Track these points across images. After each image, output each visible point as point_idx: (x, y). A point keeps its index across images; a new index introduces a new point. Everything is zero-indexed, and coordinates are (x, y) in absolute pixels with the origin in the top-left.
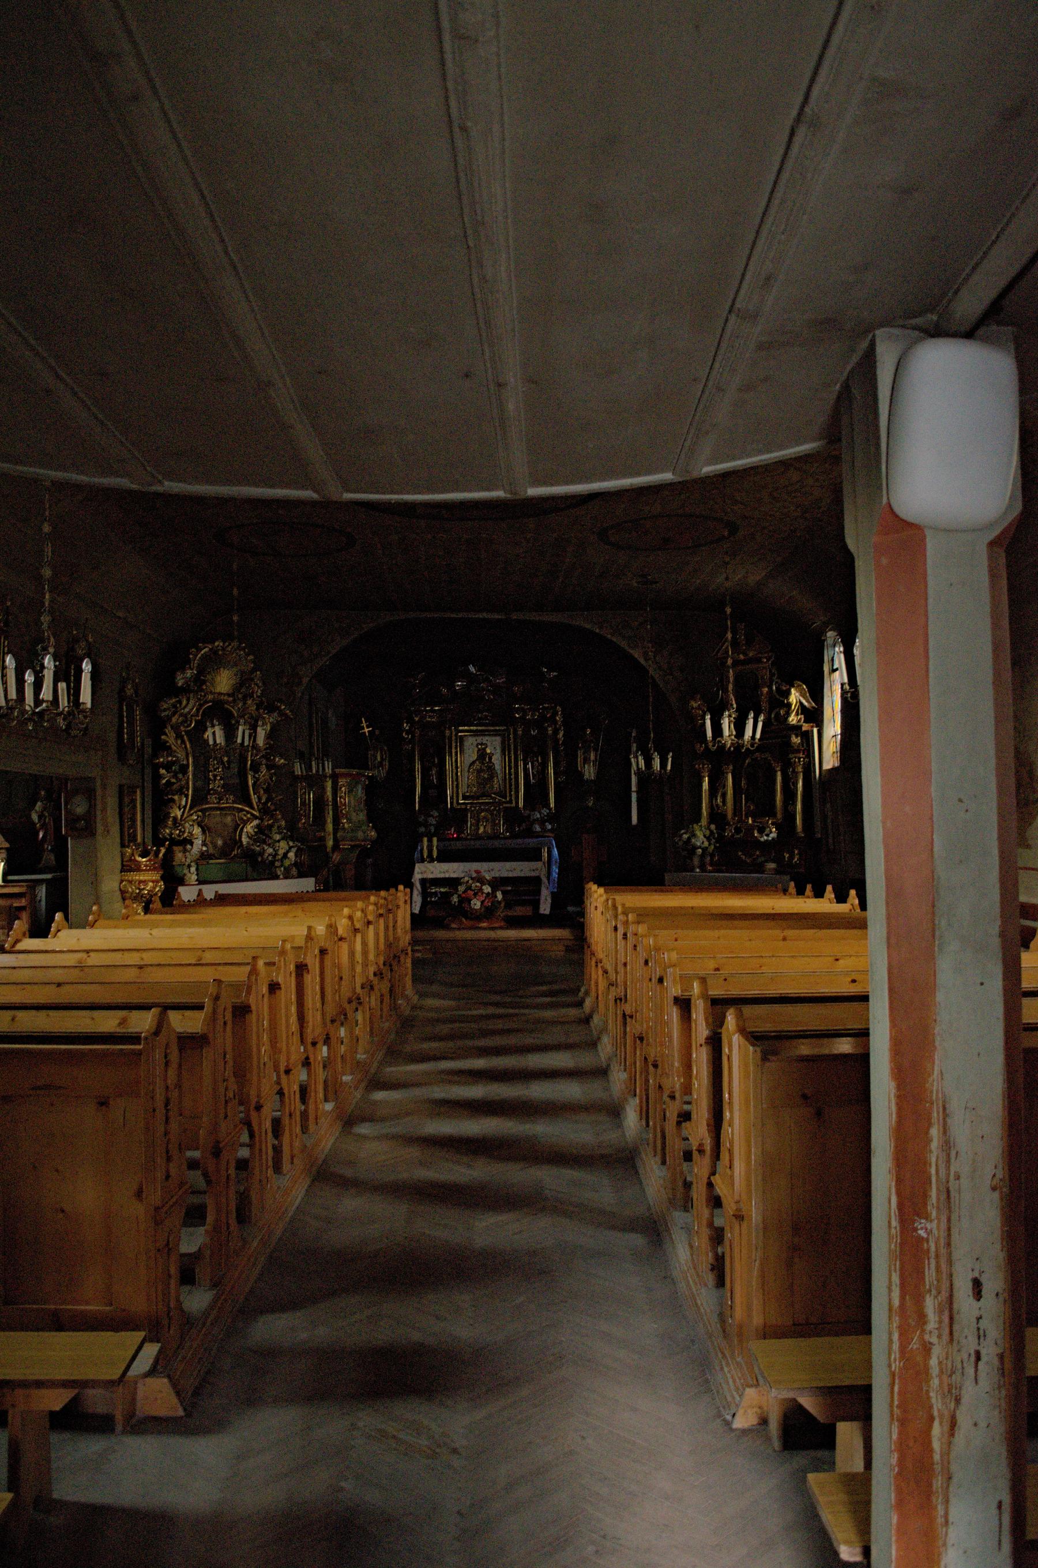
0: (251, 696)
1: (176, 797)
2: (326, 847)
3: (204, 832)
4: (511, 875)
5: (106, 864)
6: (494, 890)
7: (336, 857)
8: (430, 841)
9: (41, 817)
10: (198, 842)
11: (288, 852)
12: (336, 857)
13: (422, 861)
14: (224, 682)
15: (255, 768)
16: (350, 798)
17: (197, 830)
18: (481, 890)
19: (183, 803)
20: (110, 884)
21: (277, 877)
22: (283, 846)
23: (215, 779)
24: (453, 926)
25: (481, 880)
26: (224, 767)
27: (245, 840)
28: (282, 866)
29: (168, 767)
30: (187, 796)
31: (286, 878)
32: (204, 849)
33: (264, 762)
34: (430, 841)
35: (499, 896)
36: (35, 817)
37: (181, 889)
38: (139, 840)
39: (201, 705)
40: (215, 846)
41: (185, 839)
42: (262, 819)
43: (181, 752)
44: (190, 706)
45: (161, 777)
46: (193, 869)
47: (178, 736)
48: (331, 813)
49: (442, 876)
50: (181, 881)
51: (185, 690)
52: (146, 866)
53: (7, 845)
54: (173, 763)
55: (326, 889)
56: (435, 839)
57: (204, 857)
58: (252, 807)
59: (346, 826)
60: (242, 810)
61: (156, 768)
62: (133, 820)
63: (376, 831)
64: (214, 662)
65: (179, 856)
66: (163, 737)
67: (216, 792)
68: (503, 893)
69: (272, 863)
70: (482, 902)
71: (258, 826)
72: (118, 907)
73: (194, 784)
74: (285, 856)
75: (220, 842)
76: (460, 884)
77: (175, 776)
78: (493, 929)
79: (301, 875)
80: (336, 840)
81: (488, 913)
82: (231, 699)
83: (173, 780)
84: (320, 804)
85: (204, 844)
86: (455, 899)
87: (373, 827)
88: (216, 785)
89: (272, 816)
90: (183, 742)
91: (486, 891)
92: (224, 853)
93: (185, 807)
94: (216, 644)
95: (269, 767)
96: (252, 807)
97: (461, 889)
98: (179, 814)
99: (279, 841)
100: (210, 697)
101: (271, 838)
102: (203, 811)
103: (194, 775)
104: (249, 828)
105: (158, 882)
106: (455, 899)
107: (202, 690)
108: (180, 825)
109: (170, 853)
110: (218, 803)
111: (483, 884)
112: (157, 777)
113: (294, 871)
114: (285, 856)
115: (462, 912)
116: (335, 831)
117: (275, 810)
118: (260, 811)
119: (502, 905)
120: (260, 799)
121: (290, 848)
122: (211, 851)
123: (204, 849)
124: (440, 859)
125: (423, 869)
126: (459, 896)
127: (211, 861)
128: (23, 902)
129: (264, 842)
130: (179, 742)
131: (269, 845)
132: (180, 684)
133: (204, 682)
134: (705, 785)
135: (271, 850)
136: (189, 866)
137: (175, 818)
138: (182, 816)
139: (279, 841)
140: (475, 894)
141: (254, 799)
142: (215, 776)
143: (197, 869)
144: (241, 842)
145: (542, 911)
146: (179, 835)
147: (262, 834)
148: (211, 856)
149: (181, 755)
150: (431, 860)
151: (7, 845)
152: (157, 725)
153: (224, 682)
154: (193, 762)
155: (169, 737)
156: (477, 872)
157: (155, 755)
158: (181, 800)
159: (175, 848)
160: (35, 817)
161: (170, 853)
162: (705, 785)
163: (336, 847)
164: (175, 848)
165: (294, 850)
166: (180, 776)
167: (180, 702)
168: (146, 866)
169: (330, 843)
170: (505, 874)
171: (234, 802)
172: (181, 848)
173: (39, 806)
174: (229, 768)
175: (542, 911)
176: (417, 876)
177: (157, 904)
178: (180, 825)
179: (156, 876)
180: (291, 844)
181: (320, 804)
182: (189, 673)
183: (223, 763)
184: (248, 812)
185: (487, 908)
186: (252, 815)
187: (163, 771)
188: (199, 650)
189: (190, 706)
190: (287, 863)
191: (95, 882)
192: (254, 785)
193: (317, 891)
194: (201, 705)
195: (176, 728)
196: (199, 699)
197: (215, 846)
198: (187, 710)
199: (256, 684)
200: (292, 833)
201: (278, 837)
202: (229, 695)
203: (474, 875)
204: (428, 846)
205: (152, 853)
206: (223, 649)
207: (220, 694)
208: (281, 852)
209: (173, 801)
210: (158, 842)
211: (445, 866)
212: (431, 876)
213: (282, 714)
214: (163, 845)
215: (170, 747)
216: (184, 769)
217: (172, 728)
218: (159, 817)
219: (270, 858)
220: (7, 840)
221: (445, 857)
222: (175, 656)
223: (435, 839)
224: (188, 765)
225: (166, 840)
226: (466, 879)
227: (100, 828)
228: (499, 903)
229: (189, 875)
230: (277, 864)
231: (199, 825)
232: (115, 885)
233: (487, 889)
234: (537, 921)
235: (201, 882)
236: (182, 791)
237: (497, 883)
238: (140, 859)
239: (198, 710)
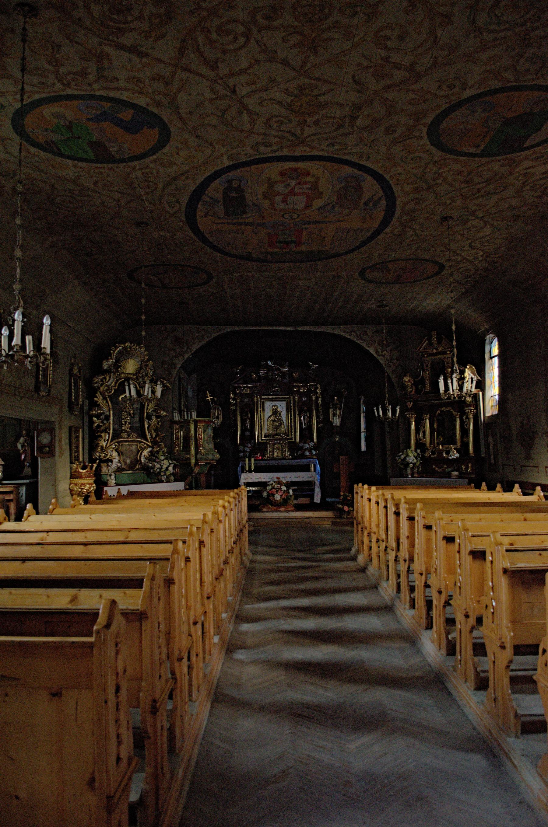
0: (147, 375)
1: (103, 434)
2: (190, 463)
3: (119, 455)
4: (297, 480)
5: (61, 474)
6: (288, 490)
7: (196, 470)
8: (250, 460)
9: (23, 446)
10: (115, 461)
11: (168, 466)
12: (196, 470)
14: (130, 367)
15: (149, 417)
16: (204, 435)
17: (115, 454)
18: (280, 489)
19: (107, 438)
20: (64, 485)
21: (162, 482)
22: (166, 463)
23: (126, 424)
24: (264, 510)
25: (280, 483)
26: (131, 417)
27: (143, 460)
28: (165, 475)
29: (98, 416)
30: (109, 434)
31: (167, 482)
32: (119, 465)
33: (154, 414)
34: (250, 460)
35: (291, 492)
36: (19, 447)
37: (105, 489)
38: (81, 459)
39: (117, 380)
40: (125, 463)
41: (108, 459)
42: (153, 447)
44: (111, 381)
45: (94, 422)
46: (113, 477)
47: (104, 398)
48: (194, 443)
49: (257, 481)
50: (106, 484)
51: (108, 371)
52: (85, 475)
53: (3, 463)
55: (191, 488)
56: (253, 460)
57: (119, 470)
58: (147, 440)
59: (202, 451)
60: (141, 442)
61: (91, 417)
62: (77, 447)
63: (220, 455)
64: (125, 355)
65: (104, 469)
66: (95, 399)
67: (126, 432)
68: (293, 490)
69: (159, 473)
70: (281, 496)
71: (151, 452)
72: (68, 500)
73: (113, 426)
74: (167, 469)
75: (128, 461)
76: (268, 485)
77: (102, 422)
78: (288, 512)
79: (176, 480)
80: (196, 459)
81: (285, 502)
82: (135, 377)
83: (101, 424)
84: (187, 438)
85: (119, 462)
86: (265, 494)
87: (217, 452)
88: (126, 427)
89: (159, 446)
90: (107, 402)
92: (131, 467)
93: (108, 440)
94: (127, 344)
95: (157, 417)
96: (147, 440)
97: (269, 488)
98: (104, 444)
99: (163, 460)
100: (123, 376)
101: (158, 459)
103: (113, 421)
105: (92, 484)
106: (265, 494)
107: (118, 371)
108: (105, 450)
109: (99, 467)
110: (127, 438)
111: (281, 485)
112: (91, 423)
113: (172, 478)
114: (167, 469)
116: (196, 454)
117: (161, 442)
118: (151, 442)
119: (293, 497)
120: (151, 435)
121: (170, 464)
122: (123, 466)
123: (119, 465)
125: (246, 477)
126: (268, 492)
128: (12, 497)
129: (155, 461)
130: (105, 402)
131: (157, 462)
132: (105, 368)
133: (119, 367)
134: (413, 427)
135: (159, 466)
136: (110, 475)
137: (102, 447)
138: (106, 445)
139: (163, 460)
140: (277, 491)
141: (148, 435)
142: (126, 422)
143: (115, 477)
144: (140, 460)
145: (315, 501)
146: (105, 457)
147: (153, 456)
148: (124, 470)
149: (106, 409)
150: (250, 471)
151: (3, 463)
152: (91, 392)
153: (130, 367)
154: (113, 414)
155: (99, 399)
156: (278, 478)
157: (90, 409)
158: (105, 436)
159: (102, 464)
160: (19, 447)
161: (99, 467)
162: (413, 427)
163: (196, 464)
164: (102, 464)
165: (172, 465)
166: (105, 422)
167: (105, 378)
168: (85, 475)
171: (137, 437)
172: (106, 464)
173: (22, 439)
174: (133, 418)
175: (315, 501)
177: (93, 498)
178: (105, 450)
179: (91, 481)
180: (170, 462)
181: (187, 438)
182: (110, 362)
183: (130, 414)
184: (145, 443)
185: (283, 499)
186: (147, 445)
187: (95, 419)
188: (116, 348)
189: (111, 381)
190: (168, 473)
191: (55, 485)
192: (148, 427)
193: (186, 489)
194: (117, 380)
195: (102, 394)
196: (117, 377)
197: (125, 463)
198: (109, 383)
199: (150, 368)
200: (170, 456)
201: (163, 458)
202: (134, 375)
203: (276, 480)
204: (249, 464)
205: (89, 467)
206: (131, 347)
207: (129, 374)
208: (165, 467)
209: (101, 436)
210: (92, 460)
211: (259, 475)
212: (250, 481)
214: (95, 463)
215: (99, 405)
216: (107, 418)
217: (101, 393)
218: (93, 447)
219: (158, 470)
220: (3, 460)
221: (258, 470)
222: (102, 352)
223: (253, 460)
224: (109, 416)
225: (97, 459)
226: (272, 482)
227: (57, 452)
228: (291, 496)
229: (110, 480)
230: (162, 474)
231: (116, 450)
232: (67, 486)
233: (284, 488)
234: (312, 507)
235: (117, 485)
236: (106, 431)
237: (289, 485)
238: (81, 471)
239: (116, 383)
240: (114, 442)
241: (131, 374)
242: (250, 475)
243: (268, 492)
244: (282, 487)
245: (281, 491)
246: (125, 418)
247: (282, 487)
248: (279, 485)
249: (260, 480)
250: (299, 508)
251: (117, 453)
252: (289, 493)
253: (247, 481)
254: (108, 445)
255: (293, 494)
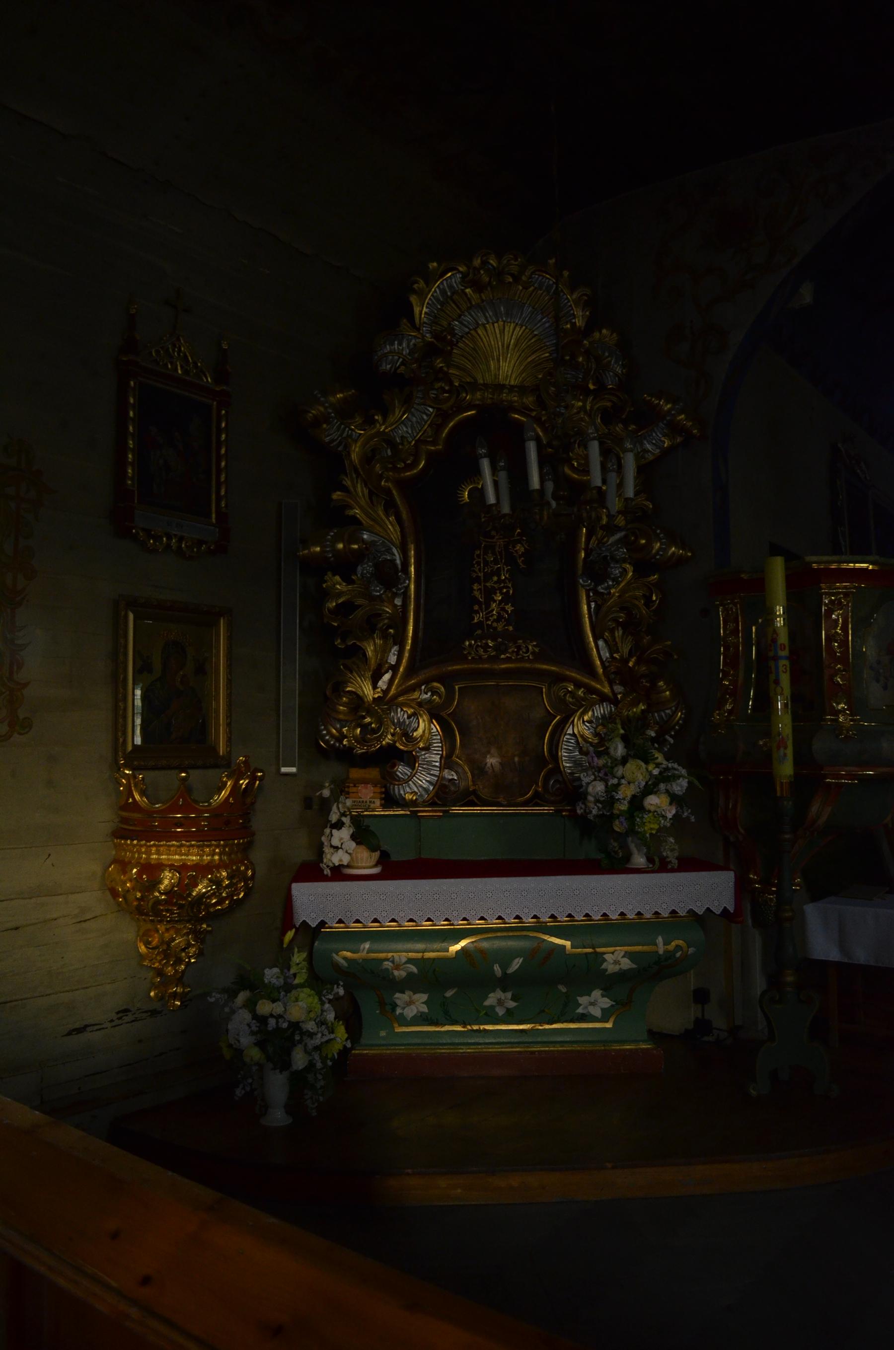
15: (598, 572)
19: (392, 659)
27: (566, 756)
32: (449, 775)
39: (444, 416)
40: (479, 770)
43: (384, 531)
44: (407, 423)
54: (360, 556)
60: (560, 679)
74: (637, 803)
75: (492, 761)
82: (529, 400)
83: (359, 601)
85: (447, 762)
93: (395, 668)
95: (643, 567)
102: (446, 679)
104: (581, 727)
114: (637, 803)
127: (457, 810)
135: (600, 787)
137: (358, 700)
144: (555, 757)
148: (469, 798)
158: (385, 651)
166: (378, 590)
169: (786, 769)
171: (538, 657)
184: (578, 685)
186: (591, 690)
194: (444, 416)
197: (479, 770)
202: (521, 389)
207: (499, 387)
208: (626, 792)
213: (674, 428)
216: (389, 576)
230: (618, 827)
231: (434, 715)
239: (437, 428)
240: (422, 676)
241: (512, 388)
246: (488, 577)
251: (436, 727)
254: (393, 691)
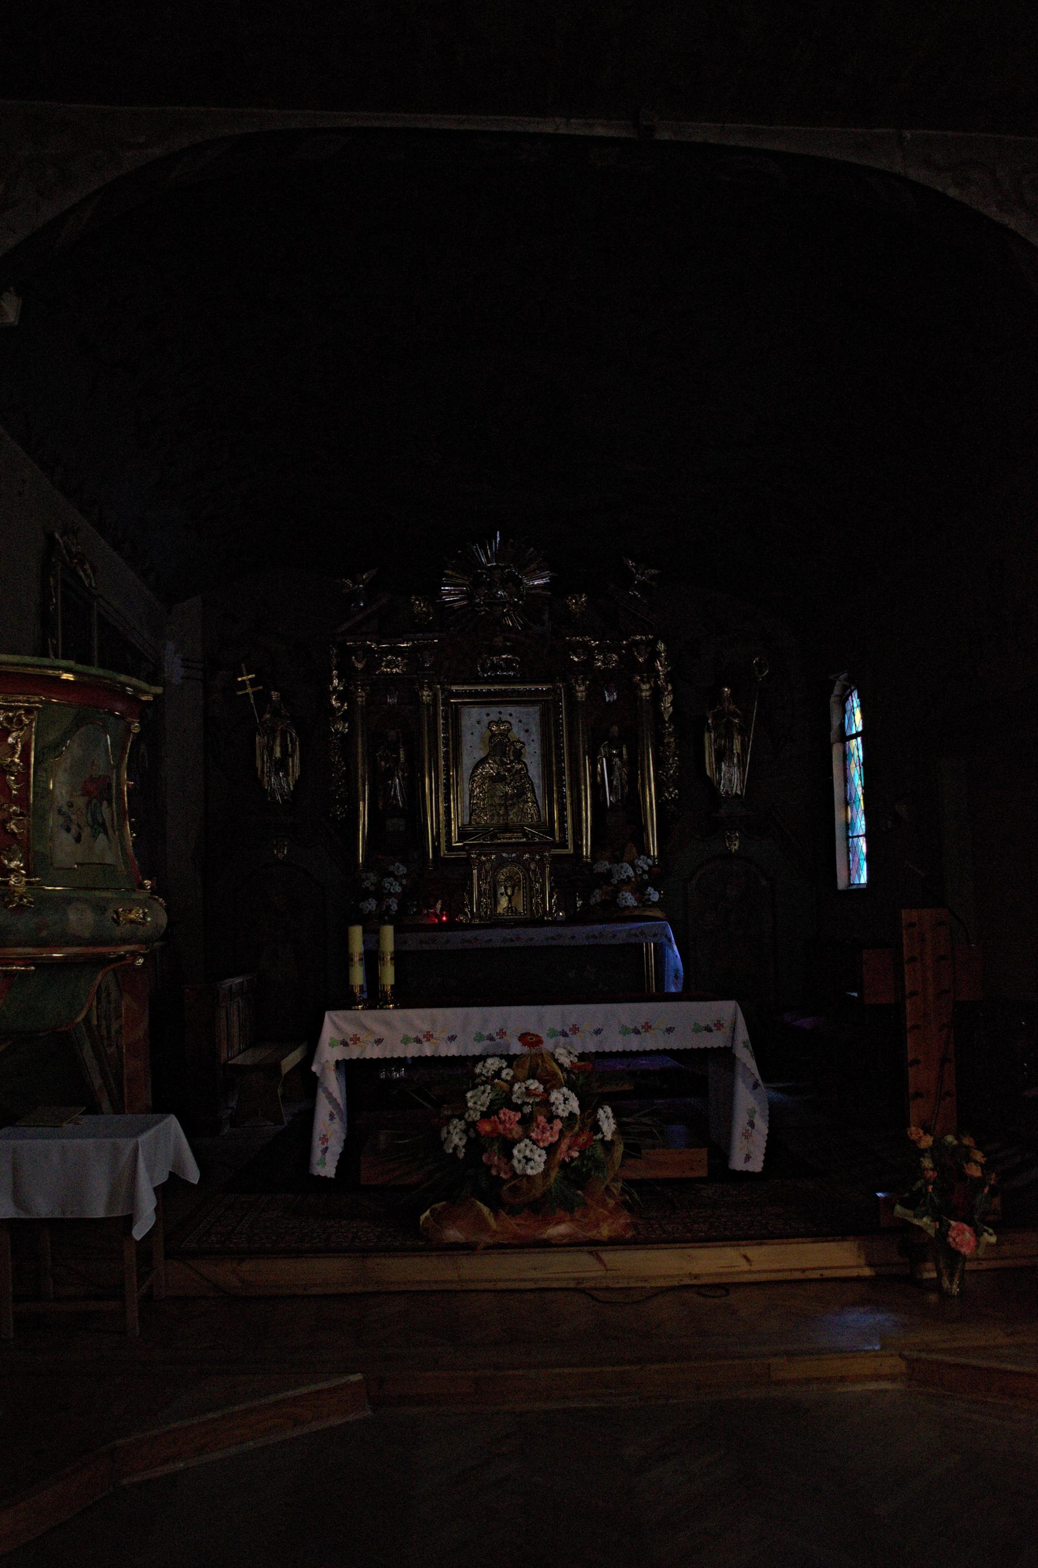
6: (589, 1105)
8: (372, 934)
13: (346, 1001)
34: (372, 934)
35: (607, 1123)
49: (412, 1051)
56: (388, 932)
76: (473, 1082)
81: (574, 1179)
86: (456, 1138)
91: (562, 1111)
97: (478, 1100)
106: (456, 1138)
111: (550, 1083)
115: (478, 1177)
124: (407, 996)
125: (350, 1030)
140: (527, 1122)
170: (616, 1043)
176: (329, 1053)
185: (563, 1165)
211: (420, 1018)
212: (374, 1052)
223: (388, 932)
226: (493, 1064)
228: (608, 1146)
237: (599, 1077)
242: (370, 1018)
243: (471, 1125)
244: (555, 1096)
245: (551, 1118)
247: (555, 1096)
248: (534, 1085)
249: (428, 1050)
250: (665, 1210)
252: (597, 1128)
253: (355, 1053)
255: (621, 1128)
